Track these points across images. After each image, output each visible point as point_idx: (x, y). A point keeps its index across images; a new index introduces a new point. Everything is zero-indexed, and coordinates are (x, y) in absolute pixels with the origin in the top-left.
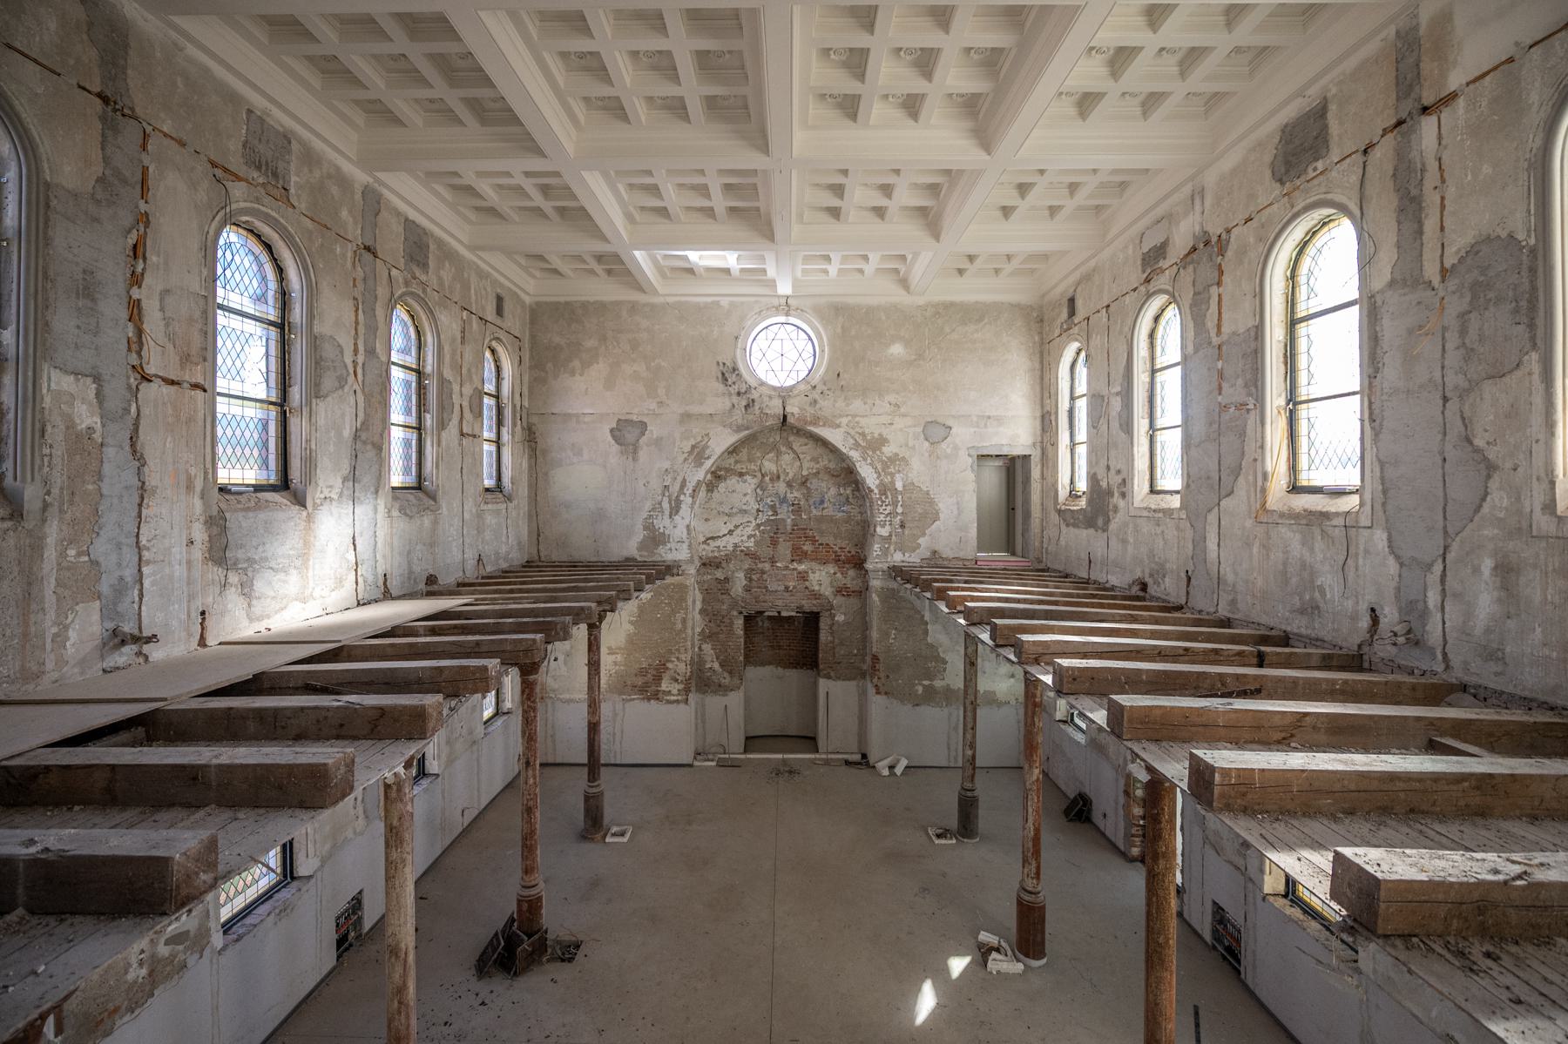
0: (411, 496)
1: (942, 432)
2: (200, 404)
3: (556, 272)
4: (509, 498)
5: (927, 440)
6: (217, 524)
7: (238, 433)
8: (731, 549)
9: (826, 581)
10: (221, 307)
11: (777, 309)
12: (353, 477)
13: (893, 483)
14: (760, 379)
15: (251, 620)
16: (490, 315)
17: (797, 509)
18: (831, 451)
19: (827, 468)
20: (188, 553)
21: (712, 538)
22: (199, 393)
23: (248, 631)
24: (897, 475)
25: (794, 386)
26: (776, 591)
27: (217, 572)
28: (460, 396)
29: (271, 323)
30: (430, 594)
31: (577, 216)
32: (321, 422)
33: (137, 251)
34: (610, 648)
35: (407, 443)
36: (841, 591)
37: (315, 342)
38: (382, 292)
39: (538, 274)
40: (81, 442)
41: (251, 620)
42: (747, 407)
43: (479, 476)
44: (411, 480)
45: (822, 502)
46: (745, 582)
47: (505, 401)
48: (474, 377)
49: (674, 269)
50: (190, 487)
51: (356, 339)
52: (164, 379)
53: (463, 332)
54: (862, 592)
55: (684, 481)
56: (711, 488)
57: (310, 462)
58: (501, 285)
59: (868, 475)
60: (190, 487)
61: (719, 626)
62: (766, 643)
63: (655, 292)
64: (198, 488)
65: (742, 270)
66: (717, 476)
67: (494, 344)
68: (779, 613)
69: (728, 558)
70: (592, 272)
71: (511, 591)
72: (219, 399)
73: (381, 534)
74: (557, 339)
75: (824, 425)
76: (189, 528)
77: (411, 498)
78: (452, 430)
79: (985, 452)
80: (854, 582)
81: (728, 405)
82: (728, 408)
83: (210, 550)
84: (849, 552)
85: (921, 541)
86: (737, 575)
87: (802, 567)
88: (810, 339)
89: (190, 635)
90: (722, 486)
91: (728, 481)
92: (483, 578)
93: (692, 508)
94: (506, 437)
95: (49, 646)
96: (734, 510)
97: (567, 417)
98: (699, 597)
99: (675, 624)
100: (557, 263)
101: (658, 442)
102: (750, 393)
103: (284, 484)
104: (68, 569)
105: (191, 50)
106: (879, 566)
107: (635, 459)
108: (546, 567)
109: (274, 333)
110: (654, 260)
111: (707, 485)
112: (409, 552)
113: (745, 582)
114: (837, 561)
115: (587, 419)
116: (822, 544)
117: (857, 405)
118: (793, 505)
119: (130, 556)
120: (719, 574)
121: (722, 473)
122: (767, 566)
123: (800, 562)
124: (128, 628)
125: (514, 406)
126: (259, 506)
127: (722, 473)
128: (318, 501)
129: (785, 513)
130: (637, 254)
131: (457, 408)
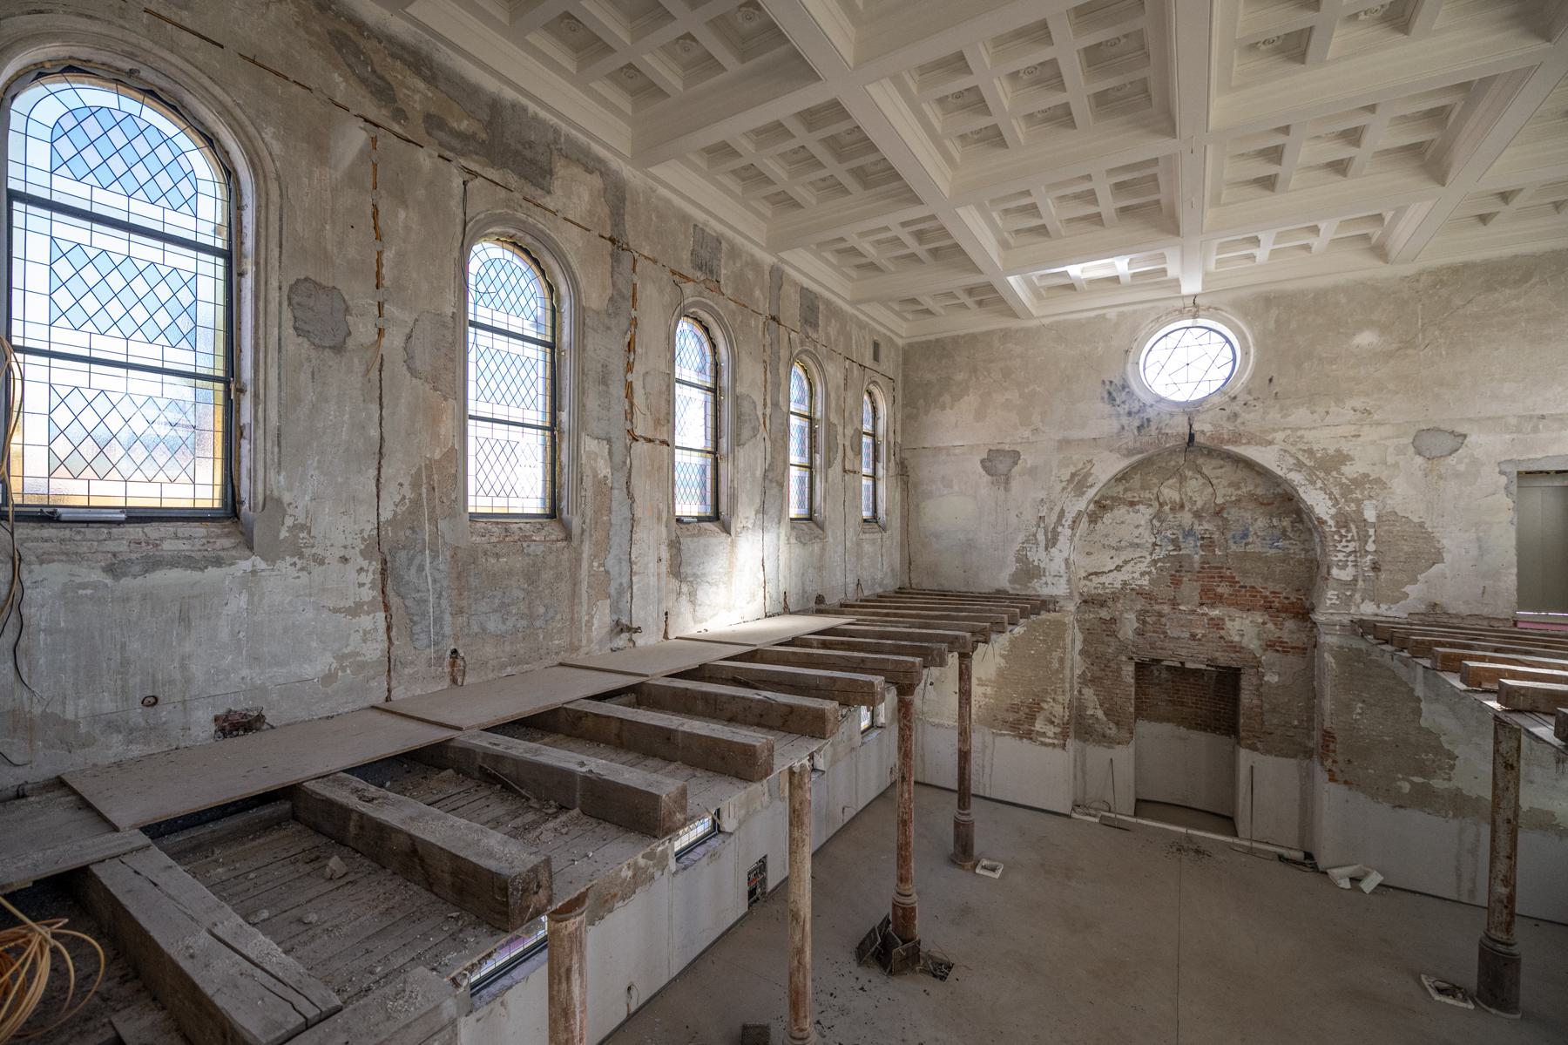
0: (804, 526)
1: (1450, 442)
3: (928, 312)
4: (884, 529)
5: (1419, 454)
6: (675, 545)
7: (688, 476)
8: (1120, 587)
9: (1251, 632)
10: (679, 381)
11: (1180, 311)
12: (762, 510)
13: (1359, 512)
14: (1157, 395)
15: (695, 622)
16: (868, 361)
17: (1208, 544)
18: (1259, 473)
19: (1253, 495)
20: (658, 568)
21: (1096, 574)
22: (665, 447)
23: (693, 630)
24: (1366, 502)
25: (1204, 399)
26: (1179, 638)
27: (674, 583)
28: (843, 438)
29: (708, 389)
30: (819, 612)
31: (950, 253)
32: (741, 465)
34: (979, 679)
35: (801, 480)
36: (1270, 645)
37: (737, 400)
38: (784, 353)
39: (910, 316)
40: (602, 488)
41: (695, 622)
42: (1139, 428)
43: (858, 508)
44: (804, 512)
45: (1245, 536)
46: (1136, 625)
47: (881, 439)
48: (855, 419)
49: (1050, 288)
50: (659, 519)
51: (765, 395)
52: (645, 439)
53: (846, 379)
54: (1308, 650)
55: (1062, 512)
56: (1094, 519)
57: (733, 498)
58: (879, 333)
59: (1319, 503)
60: (659, 519)
61: (1103, 670)
62: (1165, 697)
63: (1030, 316)
64: (664, 520)
65: (1134, 276)
66: (1102, 506)
67: (872, 387)
68: (1182, 663)
69: (1115, 597)
70: (963, 306)
71: (887, 615)
72: (676, 451)
74: (928, 376)
75: (1249, 443)
76: (659, 549)
77: (804, 527)
78: (837, 468)
79: (1534, 468)
80: (1295, 636)
81: (1116, 425)
82: (1115, 431)
83: (671, 566)
84: (1287, 598)
85: (1408, 589)
86: (1126, 615)
87: (1215, 613)
88: (1228, 341)
89: (659, 629)
90: (1108, 518)
91: (1116, 511)
92: (861, 601)
93: (1071, 540)
94: (881, 472)
95: (584, 629)
96: (1123, 544)
97: (938, 450)
98: (1079, 637)
99: (1051, 663)
100: (929, 303)
101: (1032, 471)
102: (1145, 411)
103: (716, 517)
104: (593, 575)
106: (1336, 618)
107: (1007, 490)
108: (918, 594)
109: (710, 396)
110: (1029, 283)
111: (1090, 516)
112: (803, 574)
113: (1136, 625)
114: (1268, 607)
115: (957, 451)
116: (1245, 587)
117: (1300, 415)
118: (1203, 538)
119: (626, 569)
120: (1104, 614)
121: (1108, 502)
122: (1166, 609)
123: (1213, 606)
124: (625, 620)
125: (888, 443)
126: (700, 533)
127: (1108, 502)
129: (1190, 548)
130: (1012, 280)
131: (841, 447)
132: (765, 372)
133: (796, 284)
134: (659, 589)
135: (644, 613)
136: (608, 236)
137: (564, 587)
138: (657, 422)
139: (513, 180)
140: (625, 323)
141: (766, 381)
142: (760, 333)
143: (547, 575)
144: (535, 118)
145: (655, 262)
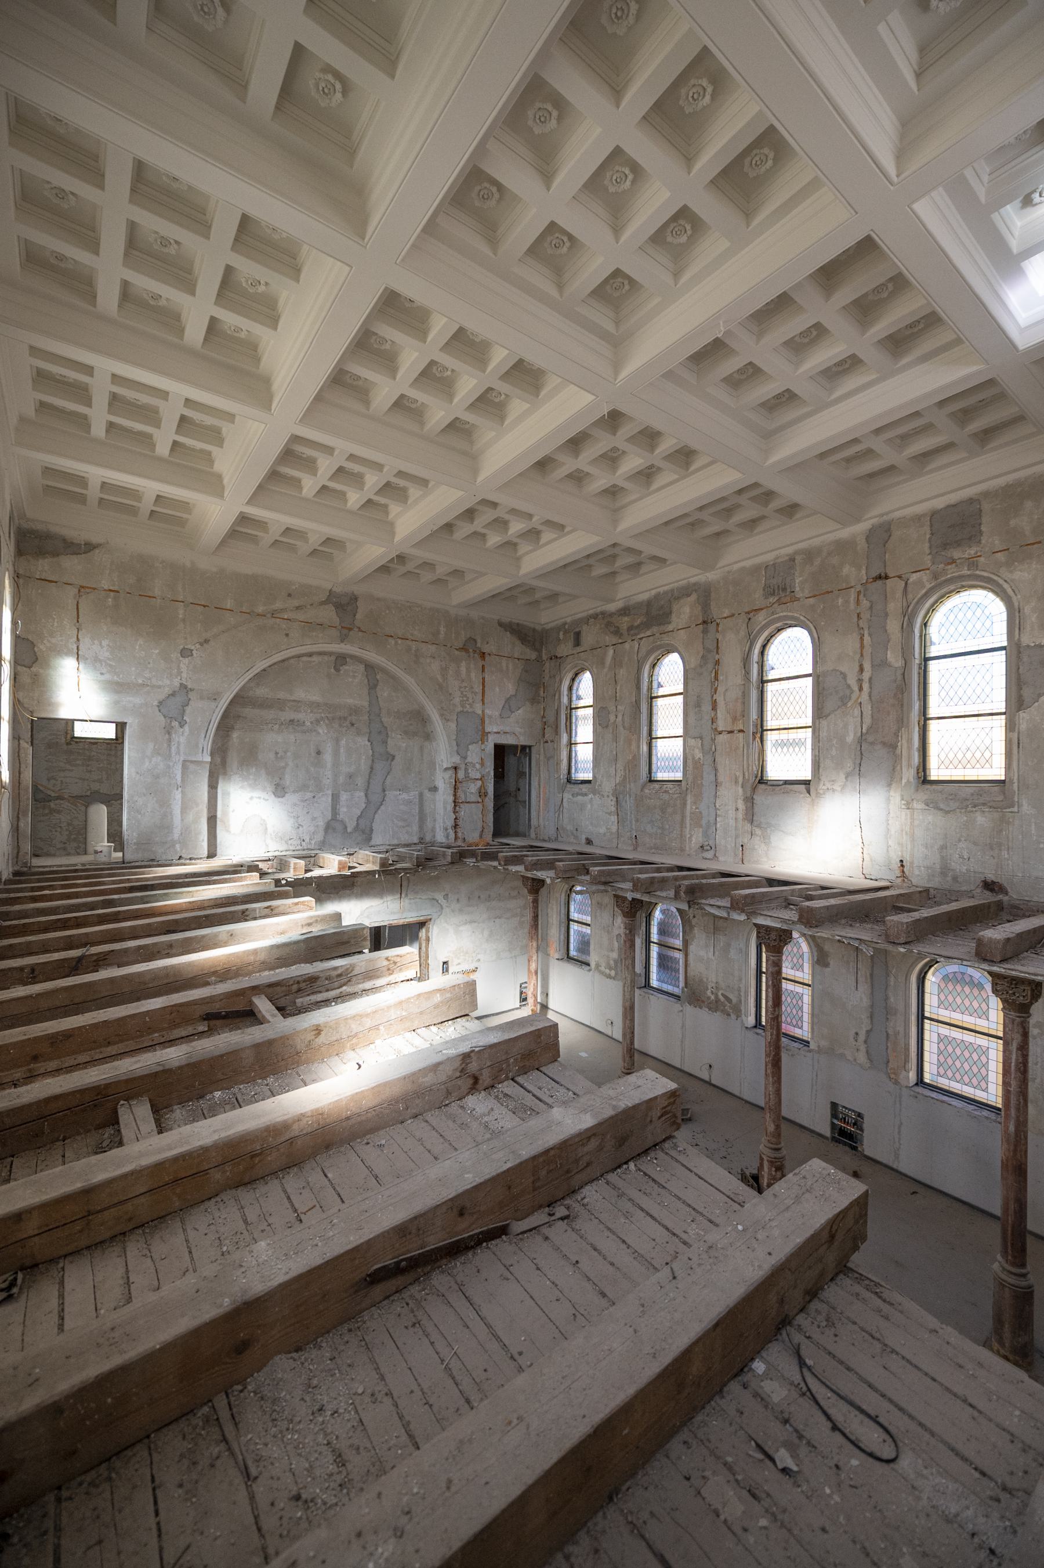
2: (741, 740)
22: (741, 734)
27: (748, 826)
33: (716, 678)
60: (736, 782)
64: (740, 783)
73: (895, 826)
83: (746, 814)
89: (736, 855)
105: (736, 567)
112: (943, 847)
128: (821, 792)
132: (862, 639)
133: (918, 519)
134: (736, 828)
135: (724, 840)
136: (700, 621)
137: (678, 818)
138: (735, 719)
139: (655, 629)
140: (710, 666)
141: (862, 647)
142: (852, 606)
143: (670, 810)
144: (666, 593)
145: (733, 615)
